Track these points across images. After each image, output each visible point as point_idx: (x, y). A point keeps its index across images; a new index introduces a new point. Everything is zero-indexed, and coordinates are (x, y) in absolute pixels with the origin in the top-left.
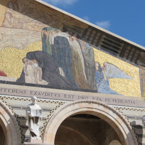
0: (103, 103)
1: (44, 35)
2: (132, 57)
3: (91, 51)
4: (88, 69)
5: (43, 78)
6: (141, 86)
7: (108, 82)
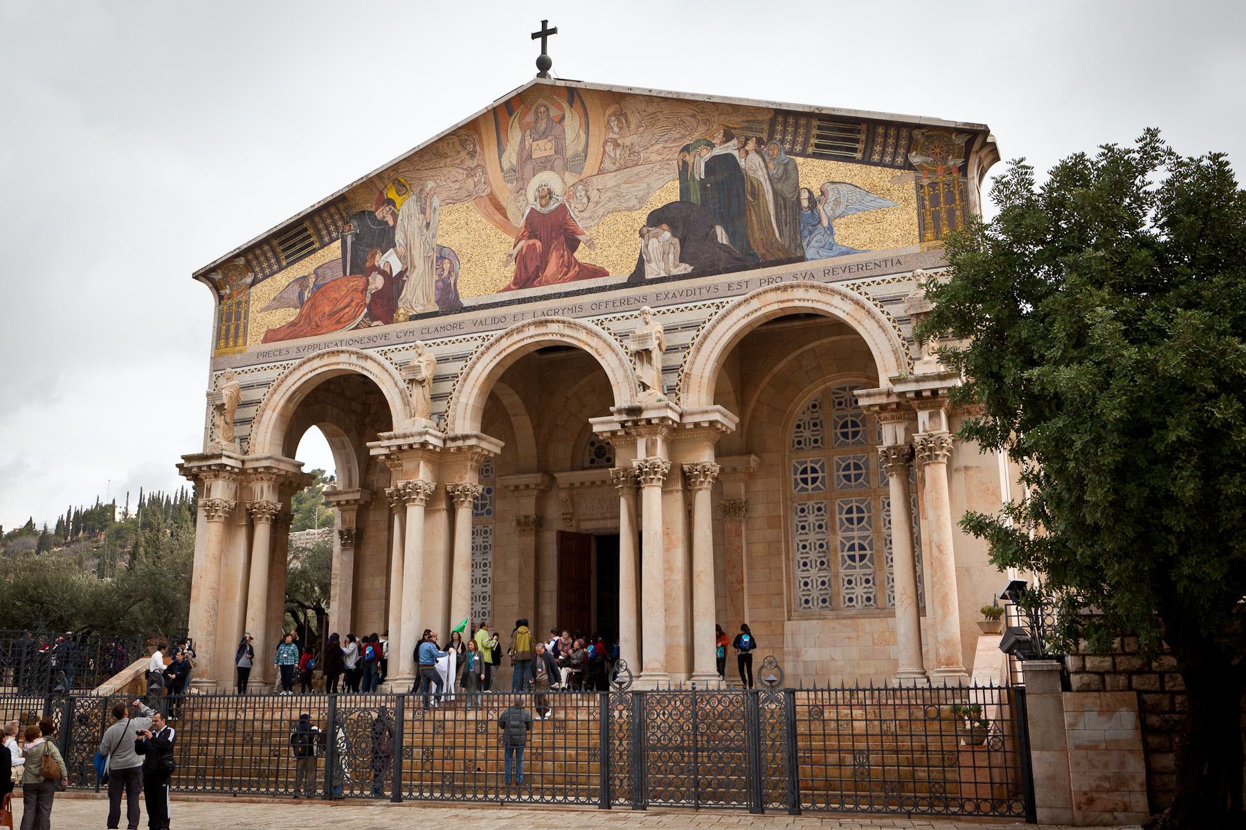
0: (815, 283)
1: (685, 163)
2: (896, 150)
3: (790, 167)
4: (783, 213)
5: (682, 260)
7: (830, 228)
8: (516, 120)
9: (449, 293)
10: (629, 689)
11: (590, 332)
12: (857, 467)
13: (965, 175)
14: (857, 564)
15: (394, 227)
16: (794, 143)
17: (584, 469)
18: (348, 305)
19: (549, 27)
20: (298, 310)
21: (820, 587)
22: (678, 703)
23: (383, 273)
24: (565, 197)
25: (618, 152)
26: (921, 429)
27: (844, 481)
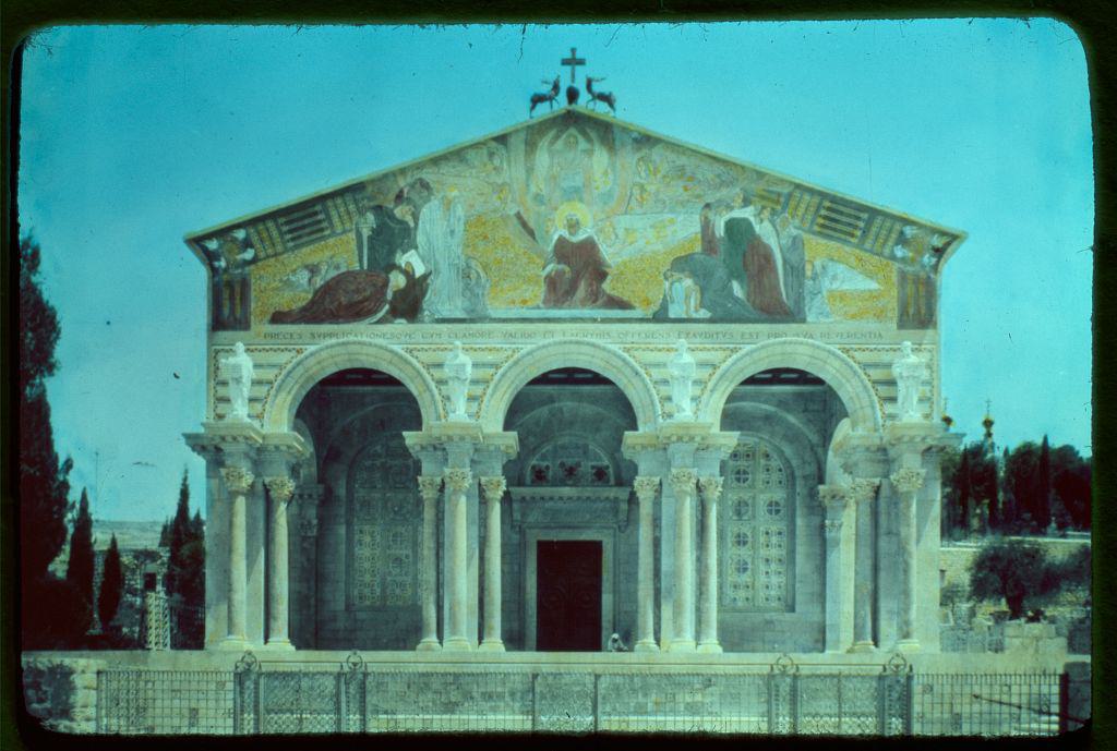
5: (702, 305)
8: (546, 144)
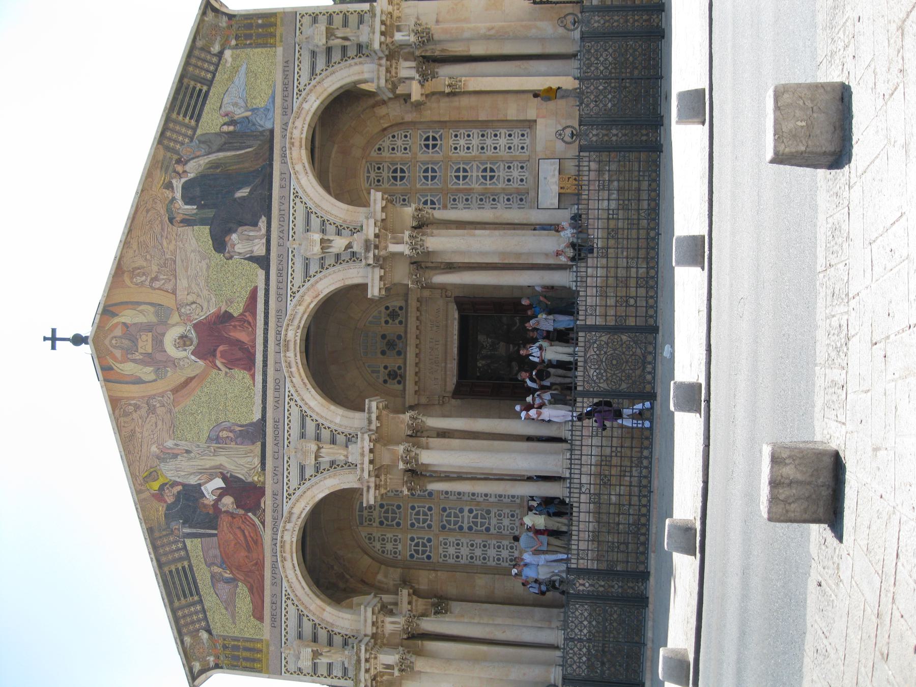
2: (207, 62)
3: (203, 139)
5: (255, 224)
6: (256, 47)
7: (253, 110)
8: (118, 365)
9: (248, 432)
10: (577, 127)
11: (300, 303)
12: (426, 171)
13: (234, 16)
14: (496, 174)
15: (184, 485)
16: (185, 135)
17: (404, 389)
18: (243, 531)
19: (50, 335)
20: (240, 584)
21: (511, 202)
22: (589, 90)
23: (220, 497)
24: (189, 323)
25: (162, 277)
26: (407, 38)
27: (436, 180)
